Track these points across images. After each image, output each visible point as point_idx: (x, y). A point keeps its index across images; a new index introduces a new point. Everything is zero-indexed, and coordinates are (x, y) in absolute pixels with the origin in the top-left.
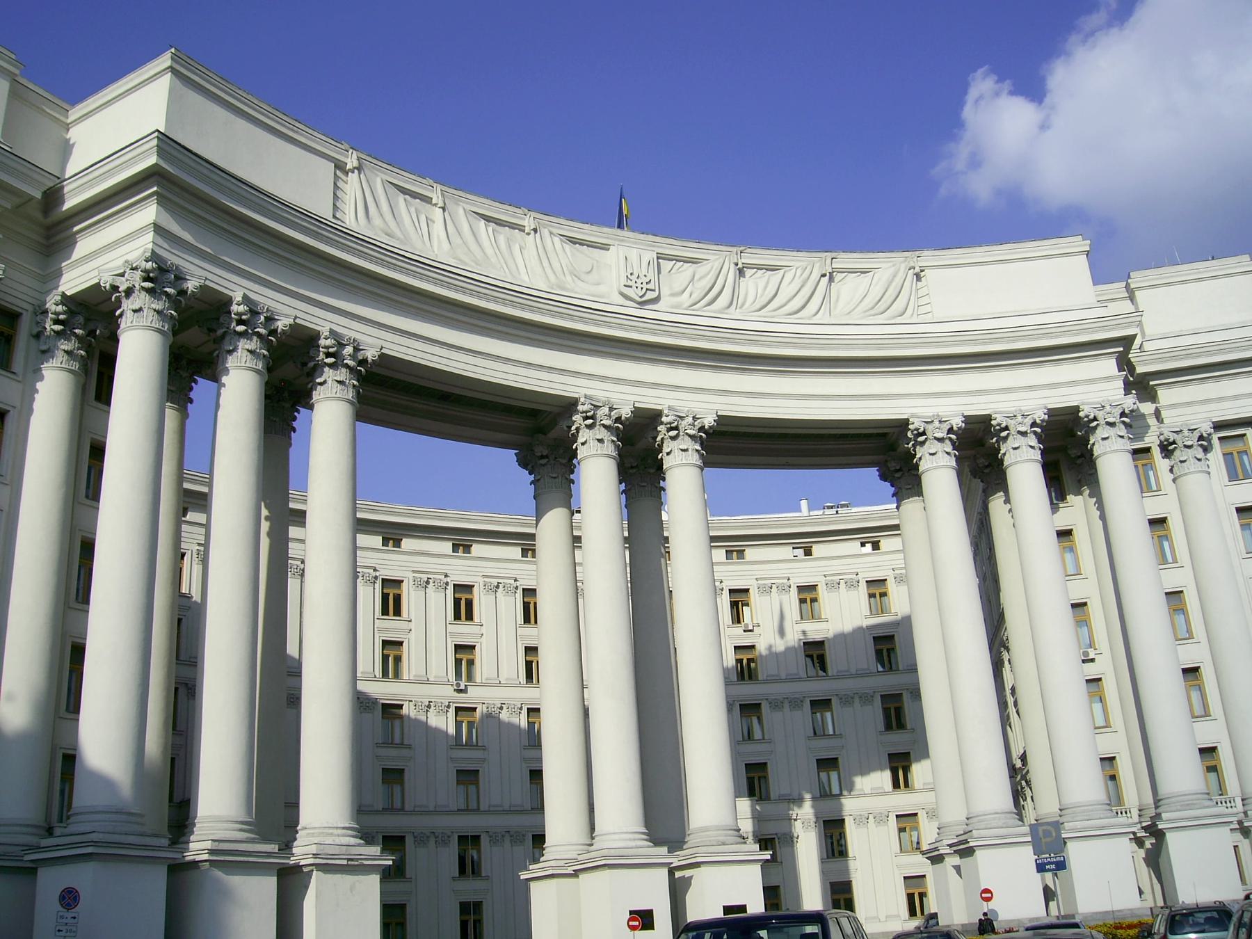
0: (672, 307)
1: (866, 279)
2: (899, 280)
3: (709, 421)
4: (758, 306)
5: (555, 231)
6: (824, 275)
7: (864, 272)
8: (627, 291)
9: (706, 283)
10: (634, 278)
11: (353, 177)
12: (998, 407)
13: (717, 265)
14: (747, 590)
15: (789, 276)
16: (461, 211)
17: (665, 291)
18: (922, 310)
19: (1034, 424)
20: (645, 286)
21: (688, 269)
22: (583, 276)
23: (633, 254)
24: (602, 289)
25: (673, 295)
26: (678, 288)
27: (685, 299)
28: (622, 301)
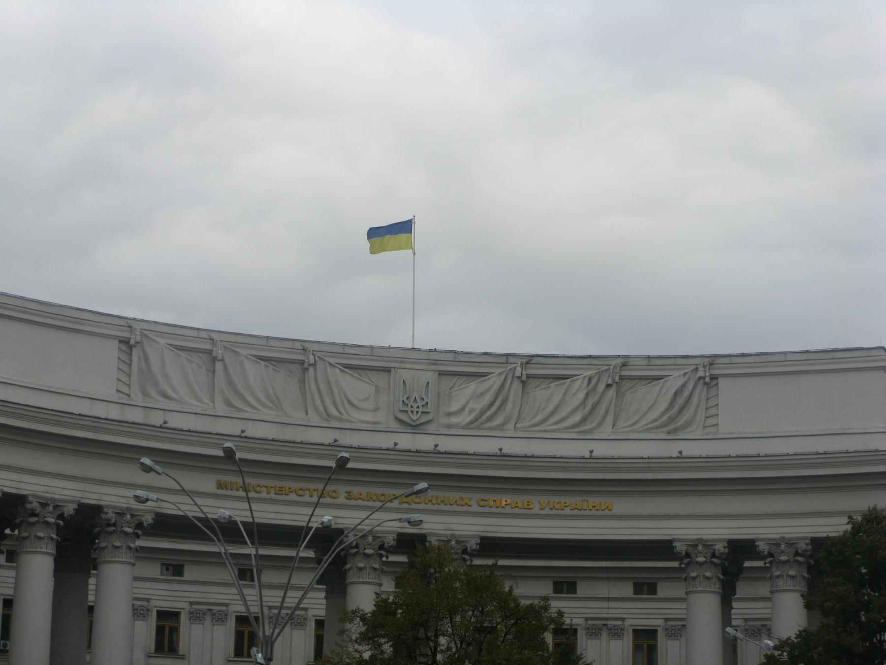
0: (449, 426)
1: (656, 387)
2: (686, 393)
3: (472, 544)
4: (539, 418)
5: (332, 361)
6: (609, 386)
7: (659, 378)
9: (487, 399)
11: (135, 353)
12: (763, 531)
13: (499, 382)
14: (655, 632)
15: (577, 384)
19: (797, 554)
20: (421, 410)
21: (473, 387)
24: (381, 416)
25: (449, 414)
26: (454, 408)
27: (464, 418)
28: (394, 425)
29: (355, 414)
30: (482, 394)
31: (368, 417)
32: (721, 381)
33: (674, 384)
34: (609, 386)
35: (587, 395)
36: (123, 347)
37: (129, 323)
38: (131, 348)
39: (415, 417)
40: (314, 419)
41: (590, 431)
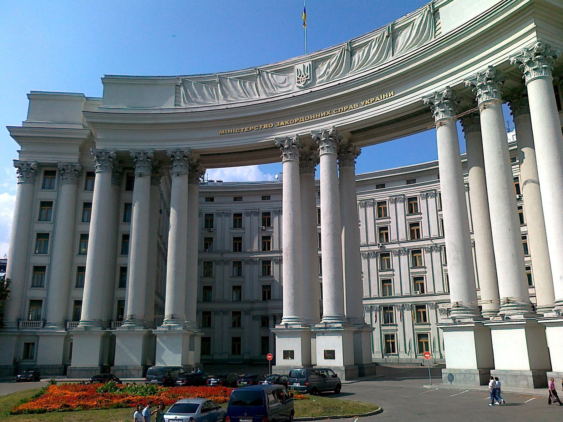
0: (319, 83)
8: (299, 85)
10: (301, 77)
16: (228, 80)
17: (318, 76)
18: (438, 32)
20: (306, 79)
21: (328, 61)
22: (281, 85)
23: (300, 67)
27: (325, 78)
29: (281, 90)
30: (333, 63)
31: (285, 90)
32: (441, 10)
33: (417, 22)
34: (388, 37)
35: (379, 46)
36: (177, 87)
37: (178, 78)
38: (180, 86)
39: (303, 83)
40: (264, 96)
41: (382, 62)
